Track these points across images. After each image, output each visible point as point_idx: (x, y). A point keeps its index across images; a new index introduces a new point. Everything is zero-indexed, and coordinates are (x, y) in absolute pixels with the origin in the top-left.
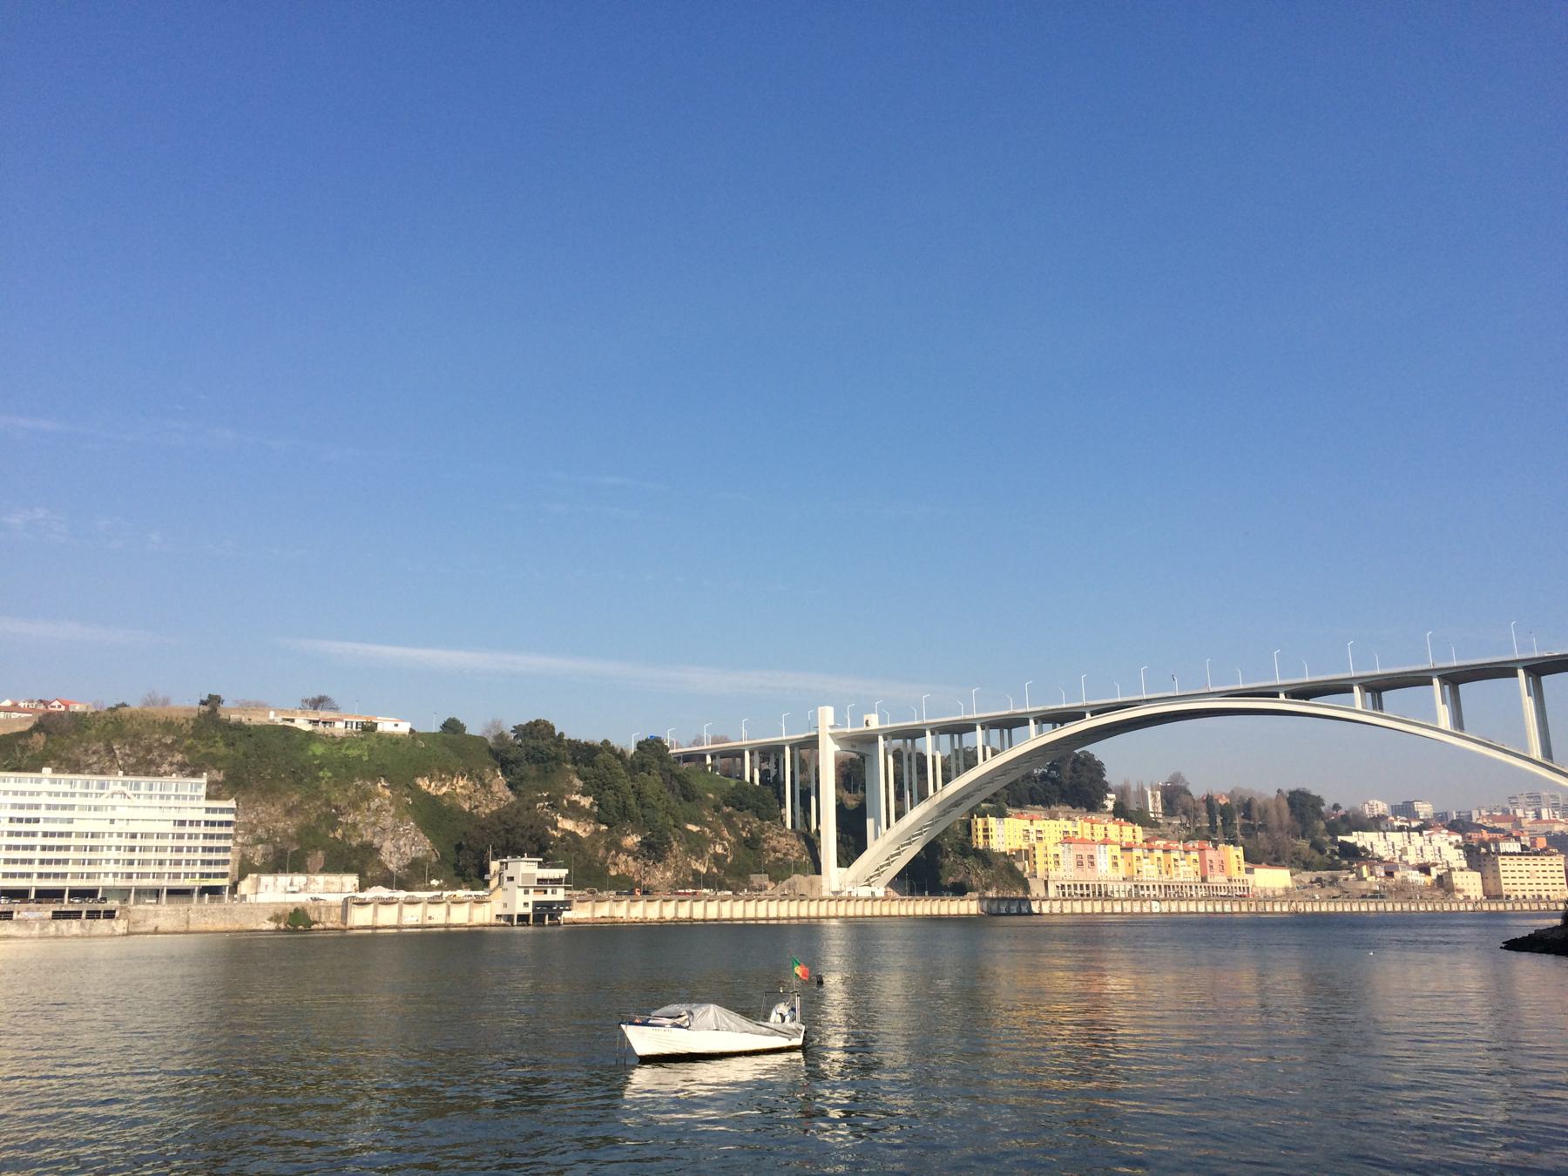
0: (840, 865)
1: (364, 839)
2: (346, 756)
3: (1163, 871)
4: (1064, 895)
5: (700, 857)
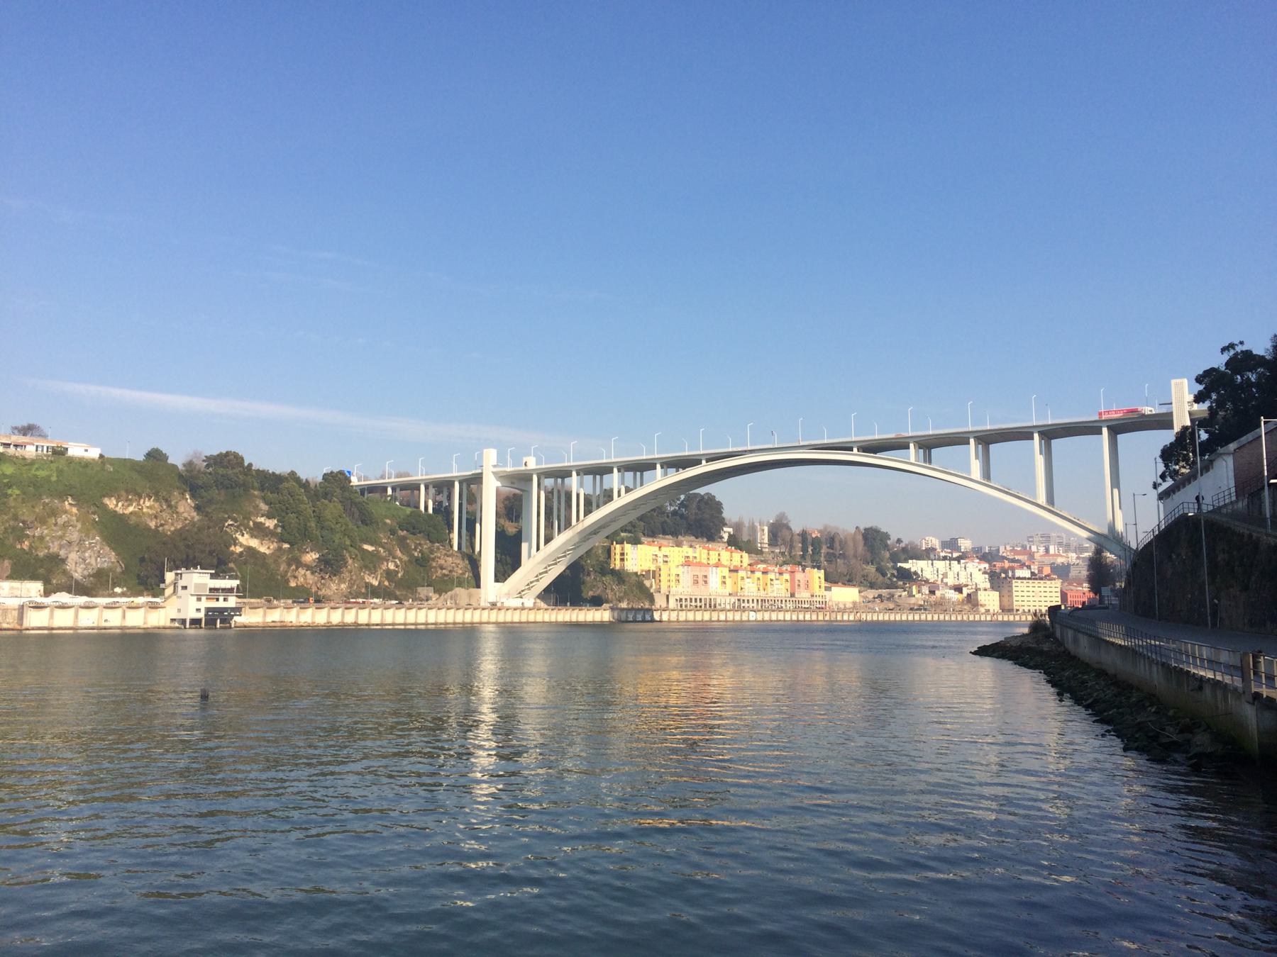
0: (497, 580)
1: (51, 550)
2: (36, 476)
3: (761, 588)
4: (681, 606)
5: (373, 571)
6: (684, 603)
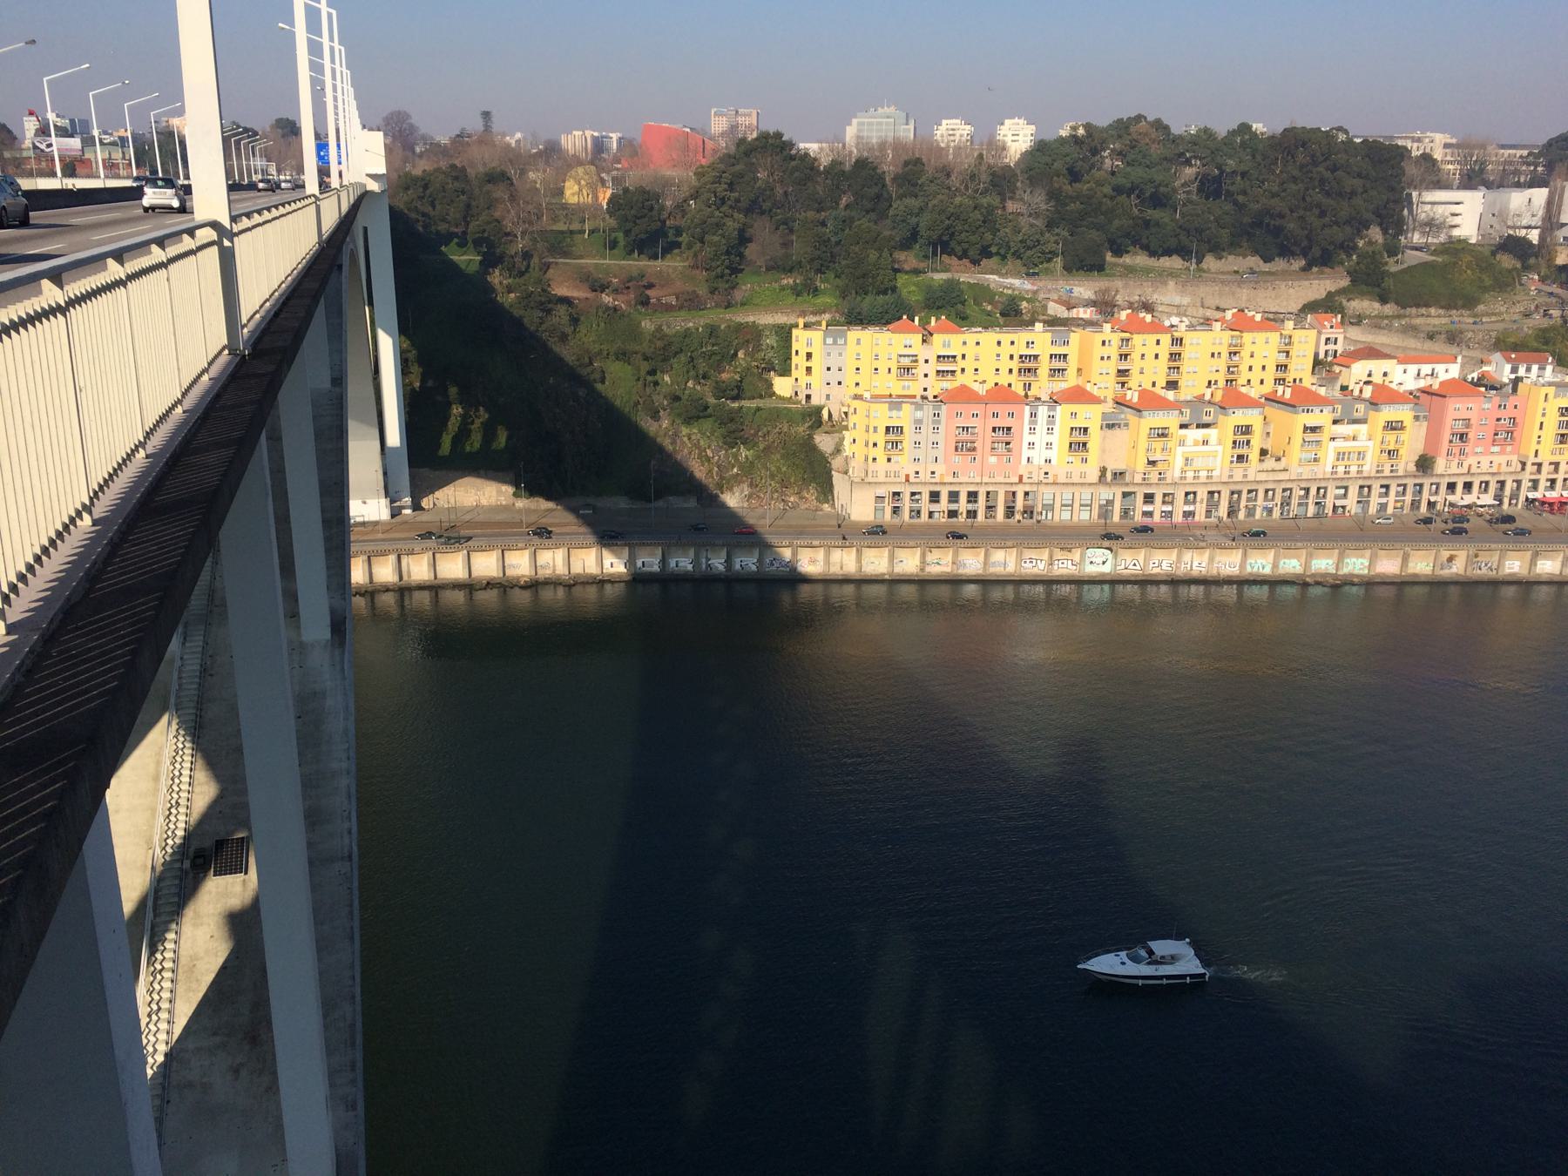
6: (906, 504)
